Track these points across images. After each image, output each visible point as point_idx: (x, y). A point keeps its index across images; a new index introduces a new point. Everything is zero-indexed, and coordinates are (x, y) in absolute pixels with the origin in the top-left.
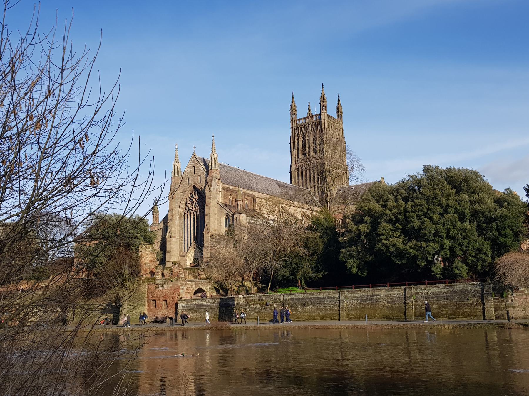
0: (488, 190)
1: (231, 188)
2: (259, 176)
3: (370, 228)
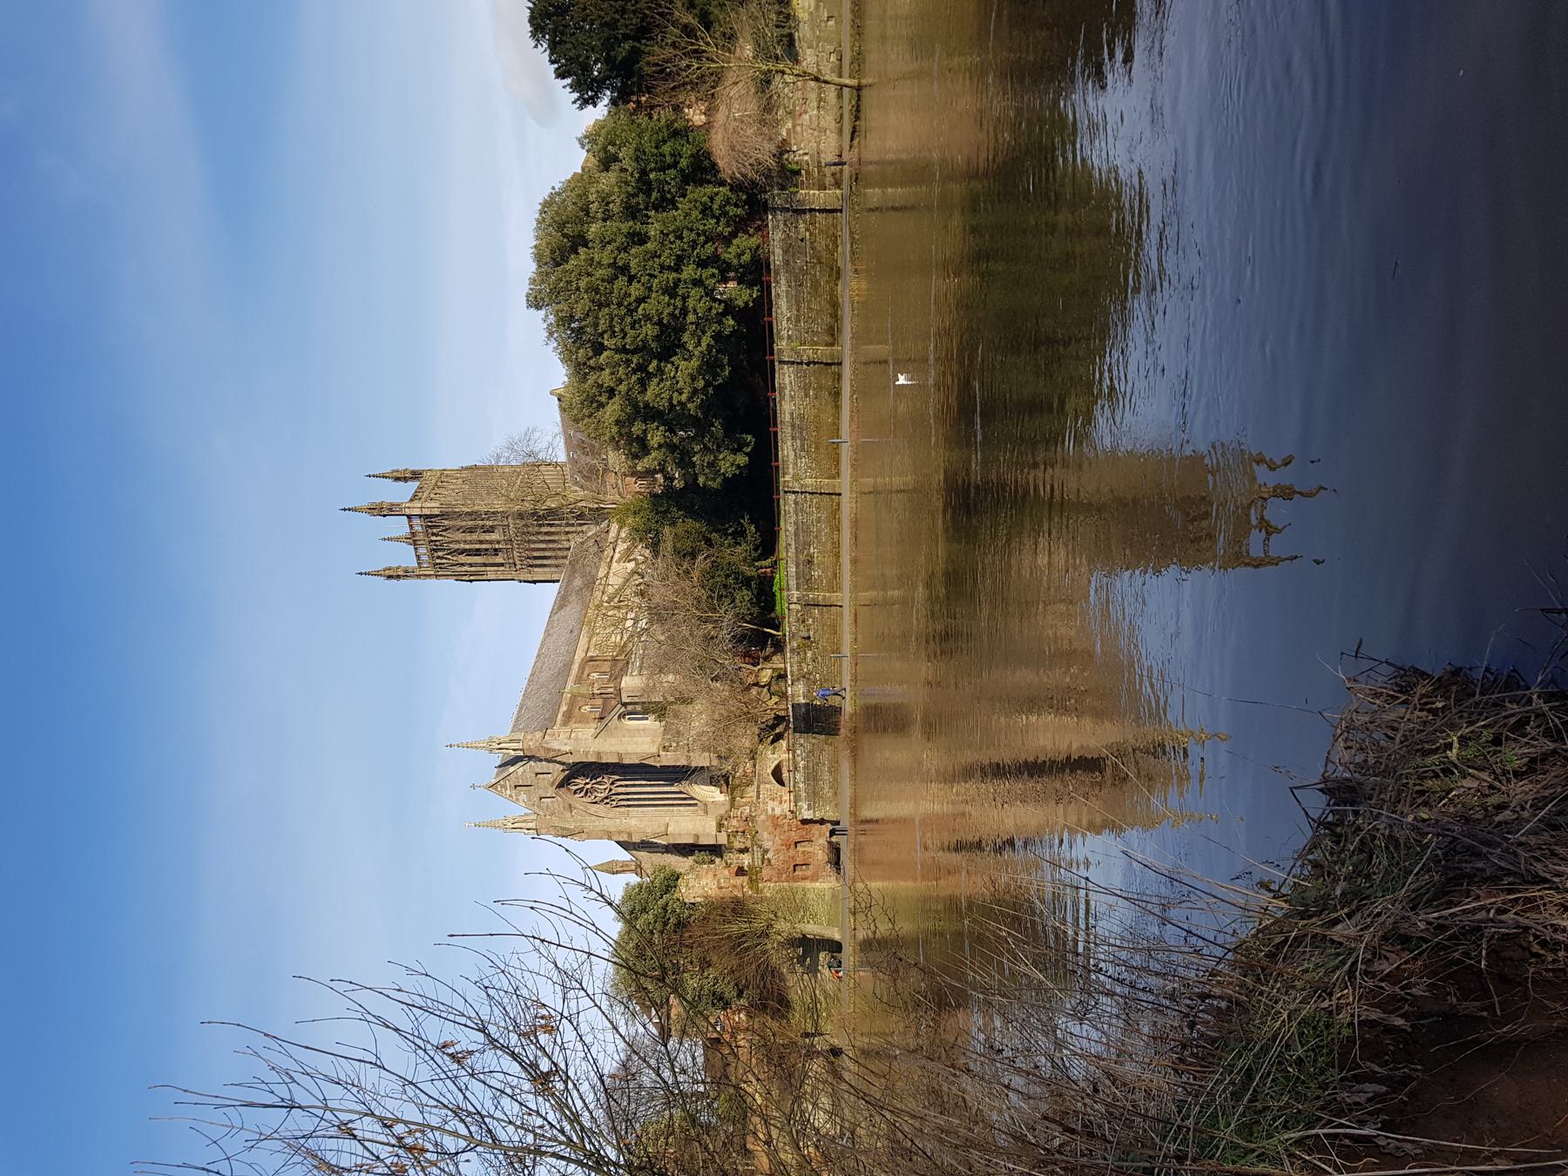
0: (580, 183)
1: (564, 708)
2: (541, 649)
3: (656, 424)
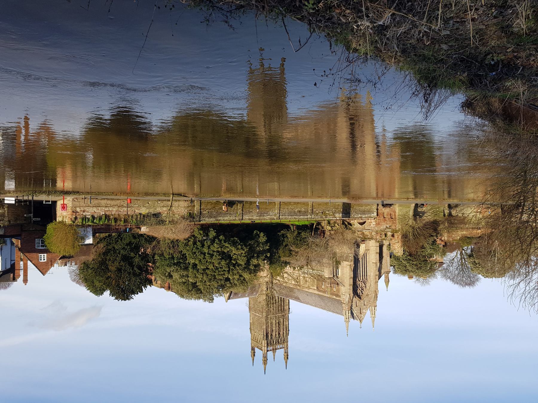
1: (334, 297)
2: (313, 306)
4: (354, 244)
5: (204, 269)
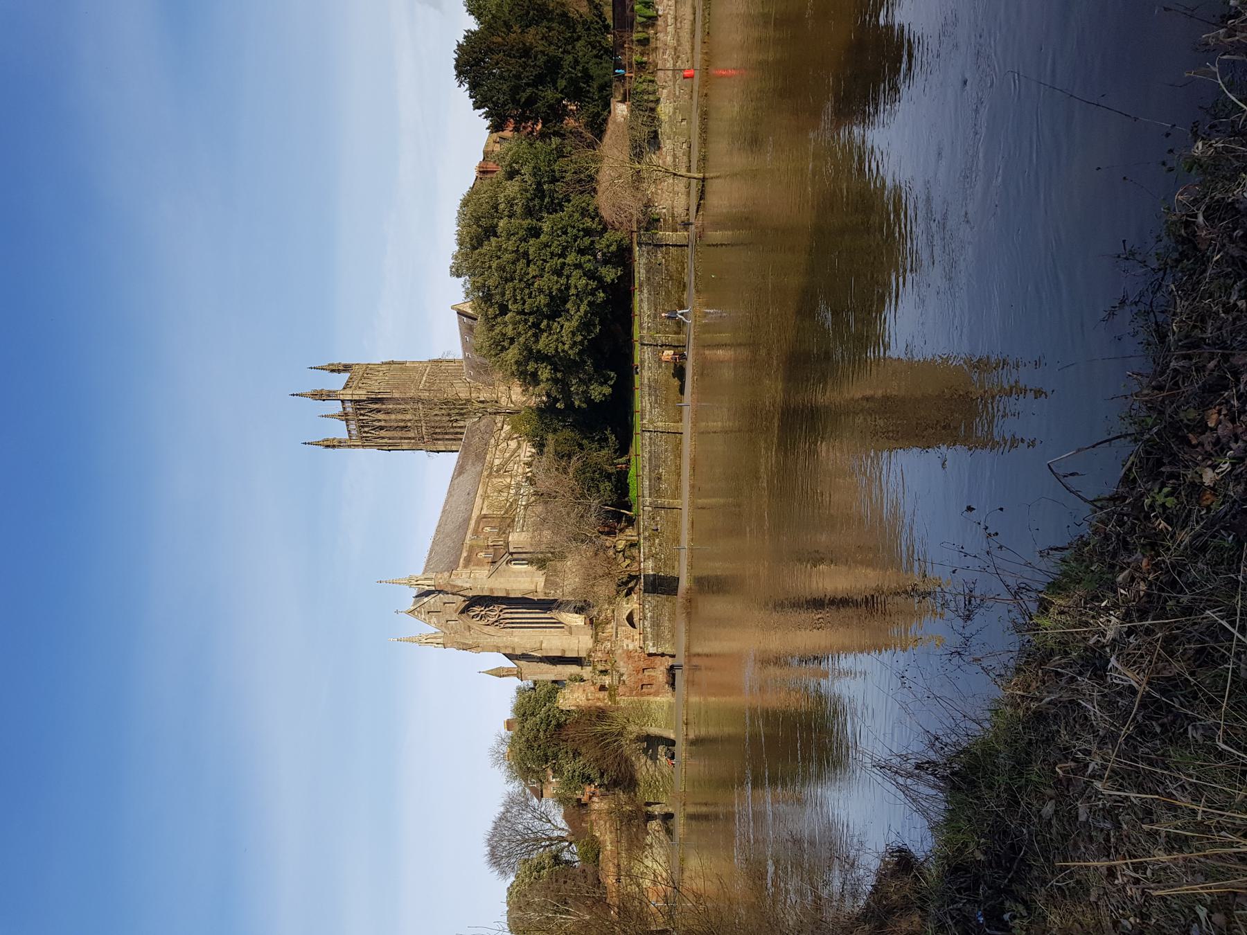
1: (465, 554)
2: (444, 507)
4: (585, 601)
5: (528, 255)
